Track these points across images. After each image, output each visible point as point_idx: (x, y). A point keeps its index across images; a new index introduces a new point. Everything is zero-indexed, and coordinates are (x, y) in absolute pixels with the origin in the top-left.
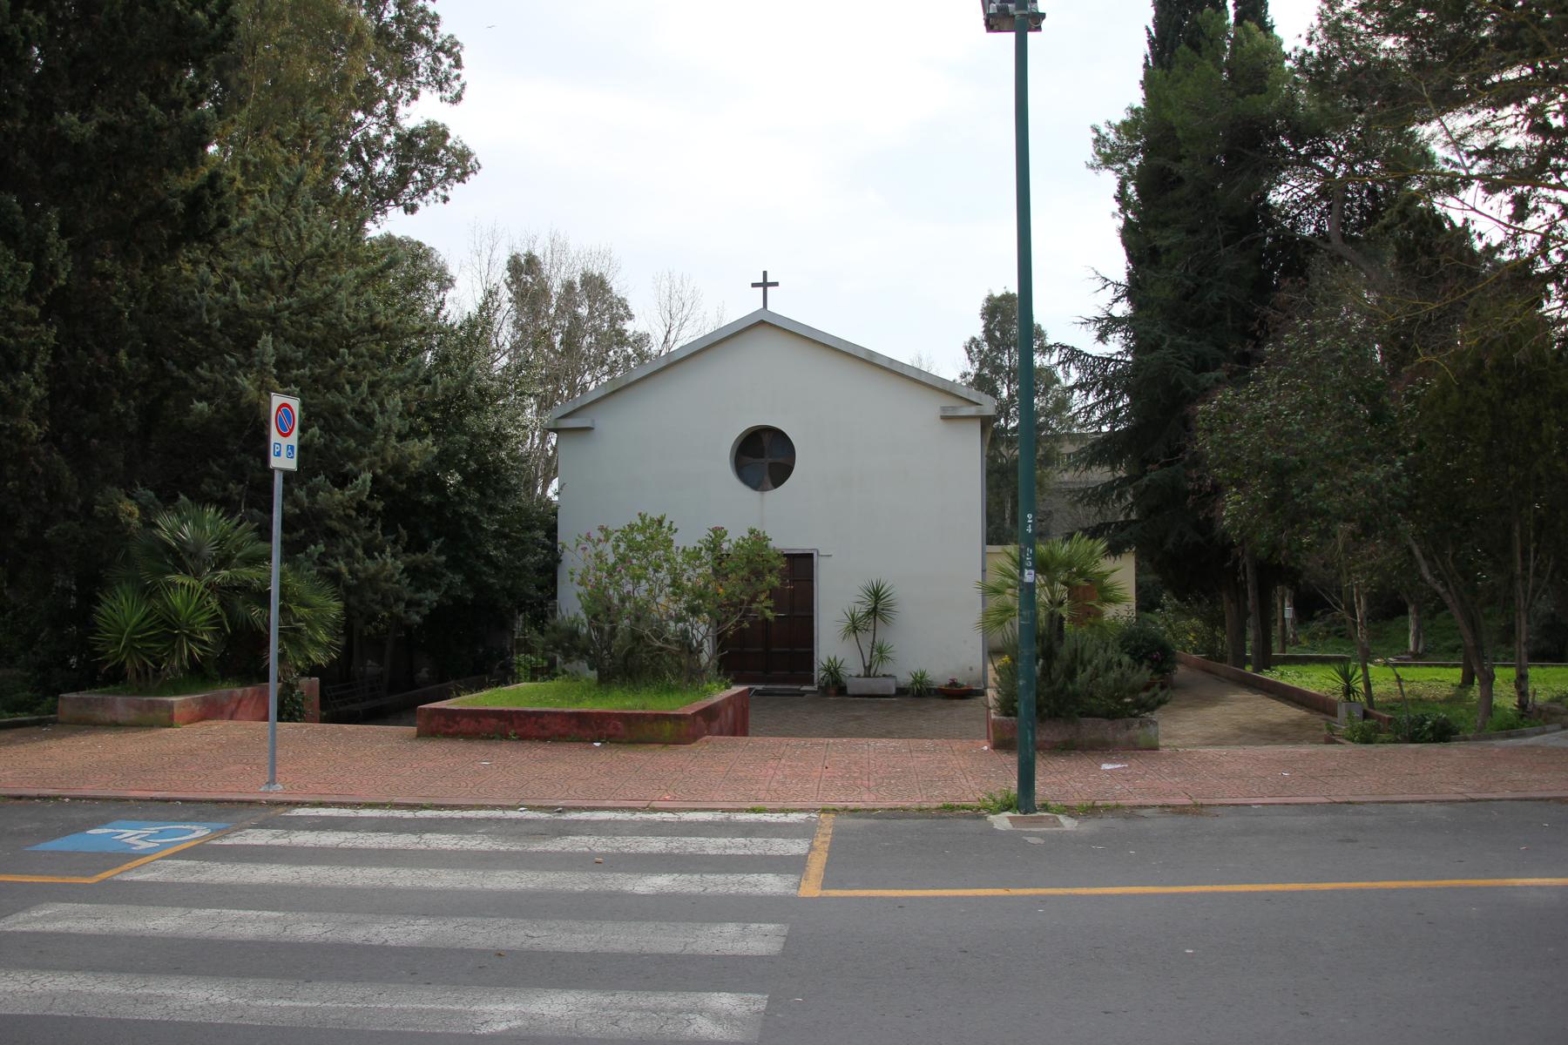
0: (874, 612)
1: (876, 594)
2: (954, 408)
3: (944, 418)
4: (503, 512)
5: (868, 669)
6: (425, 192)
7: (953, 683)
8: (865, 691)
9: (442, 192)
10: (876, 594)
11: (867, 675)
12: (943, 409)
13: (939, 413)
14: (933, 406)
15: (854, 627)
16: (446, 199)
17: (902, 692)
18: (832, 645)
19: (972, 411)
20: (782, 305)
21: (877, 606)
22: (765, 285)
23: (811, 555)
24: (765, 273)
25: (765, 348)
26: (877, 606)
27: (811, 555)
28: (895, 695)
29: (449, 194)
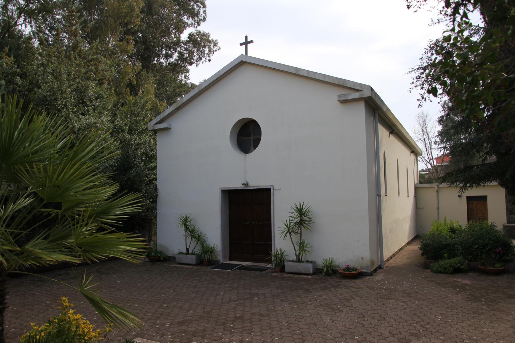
0: (300, 223)
1: (301, 212)
2: (345, 95)
3: (343, 102)
4: (47, 158)
5: (298, 256)
6: (201, 59)
7: (348, 268)
8: (294, 270)
9: (208, 58)
10: (301, 212)
11: (299, 261)
12: (339, 96)
13: (336, 99)
14: (332, 96)
15: (290, 231)
16: (210, 60)
17: (317, 271)
18: (282, 244)
19: (356, 95)
20: (254, 52)
21: (303, 219)
22: (247, 43)
23: (269, 190)
24: (246, 37)
25: (245, 75)
26: (303, 219)
27: (269, 190)
28: (313, 274)
29: (211, 59)
